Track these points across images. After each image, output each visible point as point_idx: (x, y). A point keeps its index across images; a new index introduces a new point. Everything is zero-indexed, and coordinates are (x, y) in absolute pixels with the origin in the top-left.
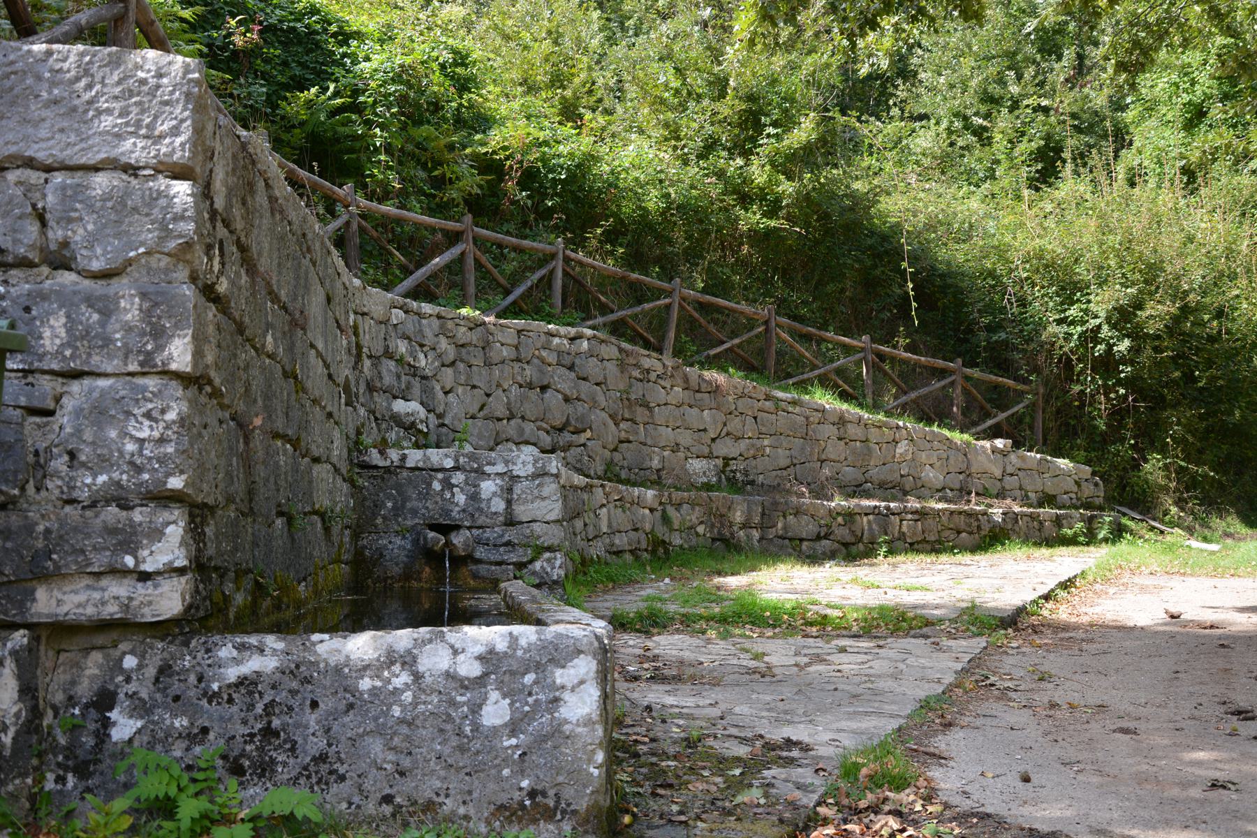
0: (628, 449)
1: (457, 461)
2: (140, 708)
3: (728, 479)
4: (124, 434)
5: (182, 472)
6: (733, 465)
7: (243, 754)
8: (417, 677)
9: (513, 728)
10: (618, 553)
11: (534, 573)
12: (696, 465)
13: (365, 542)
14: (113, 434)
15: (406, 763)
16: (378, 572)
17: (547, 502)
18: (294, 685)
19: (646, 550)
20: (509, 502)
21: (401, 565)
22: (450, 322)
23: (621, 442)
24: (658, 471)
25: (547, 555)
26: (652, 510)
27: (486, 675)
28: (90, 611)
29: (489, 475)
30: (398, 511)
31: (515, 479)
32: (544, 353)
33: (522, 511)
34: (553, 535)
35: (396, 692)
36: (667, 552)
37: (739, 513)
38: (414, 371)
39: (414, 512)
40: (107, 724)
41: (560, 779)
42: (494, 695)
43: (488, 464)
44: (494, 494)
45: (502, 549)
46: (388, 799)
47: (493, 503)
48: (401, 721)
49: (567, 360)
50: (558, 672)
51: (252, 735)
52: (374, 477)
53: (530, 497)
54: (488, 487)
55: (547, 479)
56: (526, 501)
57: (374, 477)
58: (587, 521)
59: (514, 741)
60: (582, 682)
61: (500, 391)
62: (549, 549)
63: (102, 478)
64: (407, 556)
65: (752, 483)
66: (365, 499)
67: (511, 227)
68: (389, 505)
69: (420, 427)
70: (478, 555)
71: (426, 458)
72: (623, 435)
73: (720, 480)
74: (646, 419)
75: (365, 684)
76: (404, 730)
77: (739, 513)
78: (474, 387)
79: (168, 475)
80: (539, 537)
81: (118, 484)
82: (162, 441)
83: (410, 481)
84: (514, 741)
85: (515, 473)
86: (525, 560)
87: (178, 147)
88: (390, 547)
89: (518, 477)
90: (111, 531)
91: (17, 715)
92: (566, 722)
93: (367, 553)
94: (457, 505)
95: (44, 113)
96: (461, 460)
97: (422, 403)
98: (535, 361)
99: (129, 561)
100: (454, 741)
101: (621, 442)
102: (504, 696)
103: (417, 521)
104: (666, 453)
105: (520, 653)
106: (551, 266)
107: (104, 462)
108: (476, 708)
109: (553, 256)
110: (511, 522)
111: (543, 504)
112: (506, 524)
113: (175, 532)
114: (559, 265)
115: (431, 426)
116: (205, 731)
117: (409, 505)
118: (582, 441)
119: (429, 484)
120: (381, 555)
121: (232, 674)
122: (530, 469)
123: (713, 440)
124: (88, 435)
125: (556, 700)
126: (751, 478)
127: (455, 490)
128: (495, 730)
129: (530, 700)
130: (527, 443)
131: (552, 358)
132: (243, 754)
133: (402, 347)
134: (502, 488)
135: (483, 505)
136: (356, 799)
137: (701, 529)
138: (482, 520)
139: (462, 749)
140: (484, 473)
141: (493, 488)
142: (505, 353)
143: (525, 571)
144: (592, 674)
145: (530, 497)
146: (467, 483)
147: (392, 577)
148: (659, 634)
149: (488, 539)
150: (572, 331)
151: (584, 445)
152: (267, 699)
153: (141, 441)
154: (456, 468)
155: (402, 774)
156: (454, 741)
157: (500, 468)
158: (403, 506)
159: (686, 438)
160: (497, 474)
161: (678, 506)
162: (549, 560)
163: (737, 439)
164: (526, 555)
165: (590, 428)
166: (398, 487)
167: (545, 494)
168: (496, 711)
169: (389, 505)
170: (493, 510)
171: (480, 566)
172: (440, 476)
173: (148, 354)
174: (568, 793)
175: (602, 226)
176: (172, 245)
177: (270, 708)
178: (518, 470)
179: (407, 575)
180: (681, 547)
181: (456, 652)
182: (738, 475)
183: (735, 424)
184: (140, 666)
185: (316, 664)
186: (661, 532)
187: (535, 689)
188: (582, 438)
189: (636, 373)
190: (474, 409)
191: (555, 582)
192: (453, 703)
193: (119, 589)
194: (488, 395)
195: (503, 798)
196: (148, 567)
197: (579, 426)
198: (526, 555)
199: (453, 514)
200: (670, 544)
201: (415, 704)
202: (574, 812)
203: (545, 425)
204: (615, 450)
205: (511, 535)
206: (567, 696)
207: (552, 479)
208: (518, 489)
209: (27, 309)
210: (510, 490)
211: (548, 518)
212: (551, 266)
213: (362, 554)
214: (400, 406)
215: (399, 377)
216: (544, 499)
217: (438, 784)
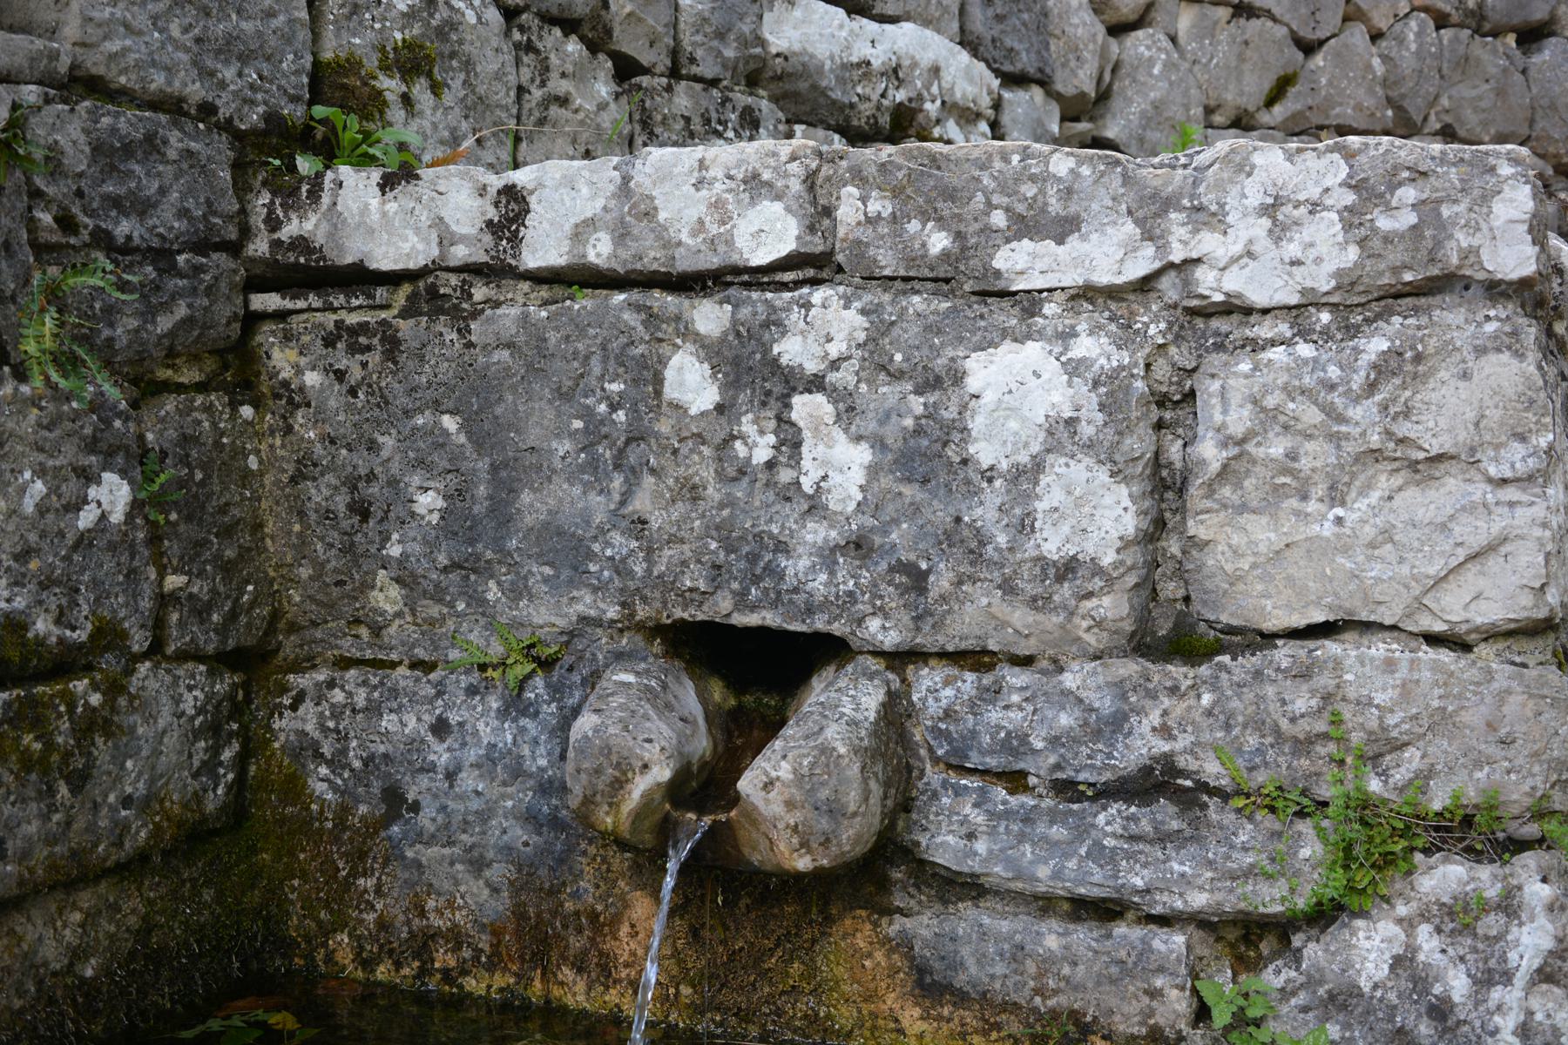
1: (820, 214)
13: (308, 719)
16: (381, 900)
17: (1452, 489)
20: (1166, 489)
21: (499, 871)
25: (1446, 876)
29: (1029, 303)
30: (475, 541)
31: (1216, 321)
33: (1253, 559)
39: (568, 552)
43: (1026, 226)
44: (1062, 433)
45: (1109, 819)
47: (1051, 494)
53: (1316, 456)
54: (1017, 388)
55: (1454, 321)
56: (1290, 483)
61: (1357, 35)
62: (1469, 832)
64: (530, 818)
66: (305, 468)
68: (428, 502)
70: (944, 844)
71: (633, 209)
83: (533, 352)
85: (1208, 283)
86: (1270, 899)
88: (441, 755)
89: (1235, 308)
93: (321, 784)
94: (815, 507)
96: (848, 209)
97: (968, 41)
103: (585, 603)
110: (1176, 636)
117: (532, 505)
119: (650, 376)
120: (395, 802)
122: (1325, 253)
127: (807, 408)
134: (1111, 390)
135: (986, 511)
138: (978, 614)
140: (995, 292)
143: (1274, 977)
145: (1316, 456)
146: (878, 365)
147: (456, 938)
149: (1016, 743)
154: (812, 266)
157: (1108, 253)
158: (502, 513)
160: (1087, 294)
162: (1458, 917)
164: (1279, 867)
166: (474, 395)
169: (428, 502)
170: (1052, 543)
171: (968, 918)
172: (709, 316)
178: (1240, 261)
179: (535, 935)
190: (1249, 89)
194: (1309, 48)
198: (1279, 867)
199: (796, 566)
205: (1176, 719)
207: (1495, 319)
208: (1230, 397)
210: (1175, 404)
211: (1456, 607)
213: (294, 787)
216: (1426, 467)
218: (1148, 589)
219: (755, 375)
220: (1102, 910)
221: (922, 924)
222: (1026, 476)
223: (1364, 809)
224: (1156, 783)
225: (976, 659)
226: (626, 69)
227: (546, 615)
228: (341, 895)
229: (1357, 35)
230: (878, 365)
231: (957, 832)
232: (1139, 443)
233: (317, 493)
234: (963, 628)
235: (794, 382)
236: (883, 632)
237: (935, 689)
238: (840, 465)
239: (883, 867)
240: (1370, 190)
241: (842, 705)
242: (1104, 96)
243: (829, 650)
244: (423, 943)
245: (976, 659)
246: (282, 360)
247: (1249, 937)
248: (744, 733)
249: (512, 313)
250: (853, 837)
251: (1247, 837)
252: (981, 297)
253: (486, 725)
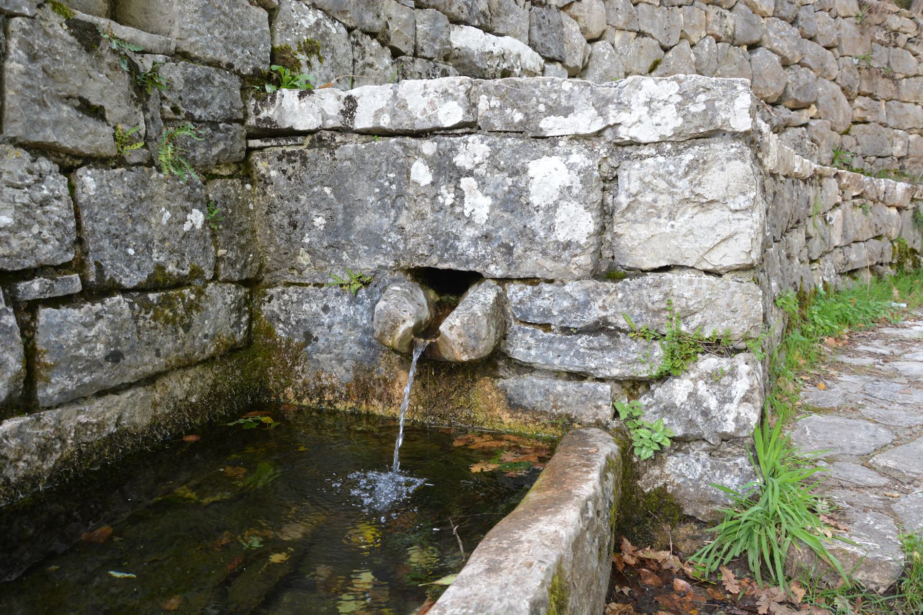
1: (472, 106)
11: (669, 409)
13: (275, 306)
16: (304, 375)
17: (717, 213)
20: (606, 214)
21: (349, 363)
25: (709, 363)
29: (554, 141)
30: (338, 237)
33: (639, 242)
34: (735, 308)
39: (374, 240)
43: (552, 110)
44: (566, 192)
45: (582, 341)
47: (561, 216)
53: (664, 201)
54: (548, 175)
55: (719, 147)
56: (654, 211)
61: (685, 45)
64: (360, 343)
68: (319, 221)
71: (398, 105)
83: (359, 161)
85: (624, 133)
86: (643, 372)
88: (326, 319)
89: (634, 143)
93: (280, 331)
94: (470, 222)
96: (483, 104)
97: (532, 45)
103: (381, 260)
110: (609, 271)
112: (596, 275)
117: (360, 222)
119: (405, 171)
120: (308, 336)
122: (670, 121)
127: (466, 183)
134: (585, 176)
135: (536, 223)
143: (644, 401)
145: (664, 201)
146: (495, 166)
147: (333, 389)
149: (547, 313)
154: (469, 127)
157: (585, 121)
158: (348, 225)
160: (576, 137)
162: (714, 378)
164: (646, 359)
166: (337, 179)
169: (319, 221)
170: (562, 235)
171: (528, 380)
172: (428, 147)
178: (637, 124)
191: (726, 438)
194: (666, 50)
198: (646, 359)
199: (462, 245)
205: (608, 303)
207: (735, 147)
208: (632, 177)
210: (610, 181)
211: (716, 260)
213: (270, 332)
216: (707, 205)
218: (599, 254)
219: (447, 170)
220: (579, 376)
221: (510, 382)
222: (551, 209)
223: (679, 337)
224: (600, 328)
225: (531, 281)
226: (396, 53)
227: (366, 265)
228: (288, 373)
229: (685, 45)
230: (495, 166)
231: (523, 347)
232: (596, 196)
233: (276, 218)
234: (526, 269)
236: (496, 270)
237: (515, 292)
238: (479, 205)
239: (495, 360)
240: (687, 97)
241: (480, 298)
242: (585, 67)
243: (474, 278)
244: (320, 391)
245: (531, 281)
246: (261, 166)
247: (635, 386)
248: (442, 309)
249: (351, 146)
250: (484, 348)
251: (635, 347)
253: (343, 308)
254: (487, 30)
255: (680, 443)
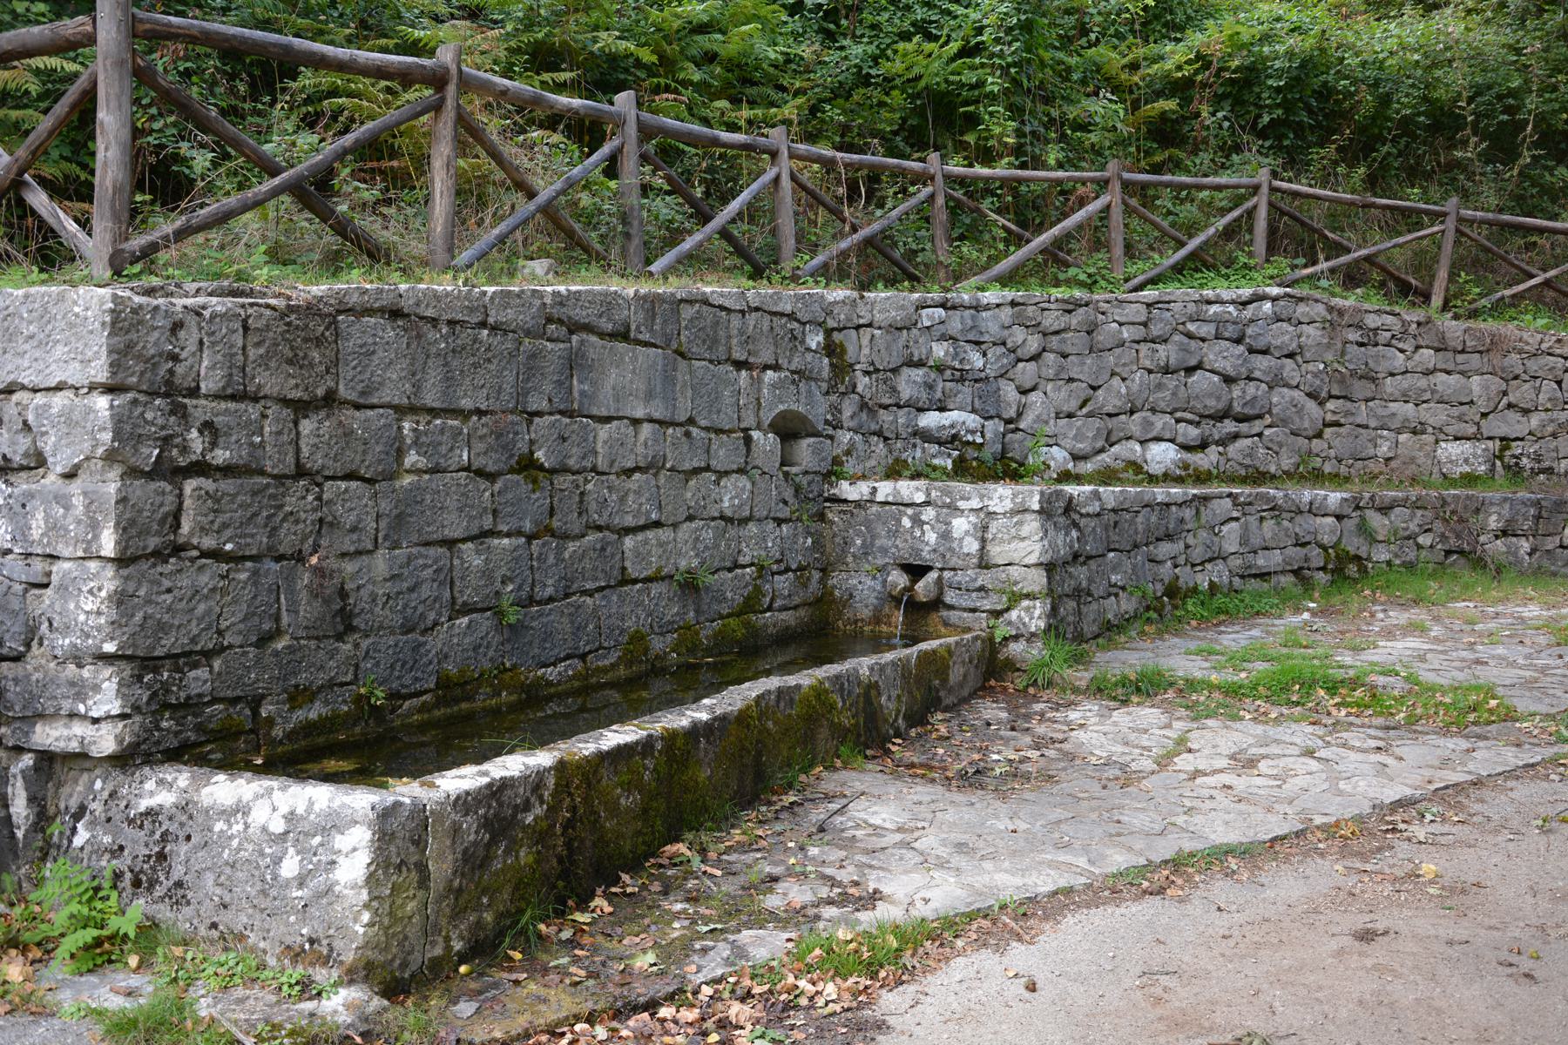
0: (1338, 435)
2: (92, 824)
3: (1507, 467)
4: (78, 606)
5: (112, 639)
6: (1517, 448)
7: (141, 871)
8: (247, 826)
9: (301, 881)
10: (1263, 576)
11: (1010, 623)
12: (1451, 450)
14: (72, 606)
15: (227, 899)
17: (1027, 542)
18: (184, 818)
19: (1323, 569)
20: (983, 541)
22: (1030, 309)
23: (1326, 425)
24: (1388, 460)
25: (1025, 603)
26: (1339, 518)
27: (287, 832)
28: (62, 744)
30: (866, 551)
32: (1191, 327)
33: (997, 553)
35: (231, 838)
36: (1363, 570)
37: (1494, 517)
38: (962, 376)
39: (884, 551)
40: (74, 830)
41: (331, 932)
42: (291, 851)
43: (962, 498)
44: (967, 533)
45: (974, 595)
46: (214, 926)
48: (227, 863)
49: (1230, 331)
50: (338, 837)
51: (150, 857)
52: (844, 512)
53: (1006, 537)
54: (960, 525)
55: (1028, 517)
56: (1002, 541)
57: (844, 512)
58: (1191, 540)
59: (300, 893)
60: (355, 850)
62: (1028, 596)
63: (67, 641)
65: (1549, 471)
67: (1205, 157)
68: (859, 542)
69: (970, 438)
71: (896, 492)
72: (1329, 417)
73: (1493, 468)
74: (1370, 395)
75: (219, 826)
76: (228, 870)
77: (1494, 517)
78: (1071, 380)
79: (103, 641)
80: (1016, 583)
81: (75, 645)
82: (99, 613)
83: (878, 515)
84: (300, 893)
85: (991, 509)
86: (999, 607)
87: (99, 371)
90: (72, 684)
91: (27, 817)
92: (337, 883)
93: (837, 593)
95: (27, 347)
96: (933, 494)
98: (1177, 338)
99: (82, 708)
100: (259, 886)
101: (1326, 425)
102: (298, 853)
104: (1403, 438)
105: (312, 817)
106: (1249, 204)
107: (66, 630)
108: (277, 861)
109: (1256, 189)
110: (984, 564)
111: (1022, 545)
112: (980, 566)
113: (110, 687)
114: (1262, 201)
115: (988, 436)
116: (121, 848)
117: (878, 543)
118: (1256, 430)
119: (899, 521)
120: (851, 596)
121: (144, 804)
122: (1008, 505)
123: (1484, 415)
124: (57, 608)
125: (334, 862)
126: (1547, 464)
127: (926, 527)
128: (288, 881)
129: (315, 859)
130: (1158, 439)
131: (1206, 330)
132: (141, 871)
133: (940, 351)
134: (975, 525)
135: (955, 545)
136: (195, 922)
137: (1425, 540)
139: (264, 893)
141: (966, 526)
142: (1126, 335)
144: (364, 843)
145: (1006, 537)
146: (938, 521)
148: (1138, 704)
150: (1246, 292)
151: (1260, 435)
152: (164, 828)
153: (87, 613)
154: (927, 503)
155: (225, 907)
156: (259, 886)
157: (975, 503)
158: (872, 545)
159: (1435, 415)
161: (1384, 510)
162: (1027, 609)
163: (1526, 412)
165: (1269, 412)
166: (868, 523)
167: (1023, 533)
168: (290, 867)
171: (952, 613)
172: (910, 511)
173: (89, 542)
174: (338, 944)
175: (1334, 142)
176: (100, 451)
177: (165, 834)
178: (995, 505)
179: (877, 619)
180: (1389, 563)
181: (274, 810)
182: (1525, 460)
183: (1521, 393)
184: (103, 789)
185: (196, 803)
186: (1354, 544)
187: (320, 850)
188: (1257, 426)
189: (1354, 336)
191: (1033, 635)
192: (262, 854)
193: (79, 729)
195: (289, 940)
196: (95, 714)
197: (1248, 411)
200: (1369, 559)
201: (238, 850)
202: (341, 962)
203: (1189, 416)
204: (1319, 435)
205: (984, 578)
206: (341, 860)
207: (1034, 516)
208: (994, 527)
209: (24, 506)
210: (985, 528)
211: (1027, 561)
212: (1249, 204)
213: (832, 594)
214: (931, 420)
215: (930, 387)
217: (245, 920)
218: (981, 558)
219: (917, 521)
220: (974, 610)
221: (945, 613)
222: (961, 540)
224: (981, 589)
225: (954, 569)
226: (886, 439)
227: (880, 562)
228: (841, 613)
229: (1116, 381)
230: (938, 521)
231: (950, 597)
232: (979, 534)
233: (837, 540)
234: (952, 564)
235: (924, 523)
236: (938, 565)
237: (947, 574)
238: (931, 537)
240: (1015, 495)
241: (933, 575)
242: (1020, 415)
243: (930, 568)
244: (856, 622)
245: (954, 569)
246: (830, 515)
247: (997, 614)
248: (914, 581)
250: (932, 596)
251: (995, 598)
252: (954, 509)
253: (869, 582)
254: (942, 409)
255: (1016, 638)
